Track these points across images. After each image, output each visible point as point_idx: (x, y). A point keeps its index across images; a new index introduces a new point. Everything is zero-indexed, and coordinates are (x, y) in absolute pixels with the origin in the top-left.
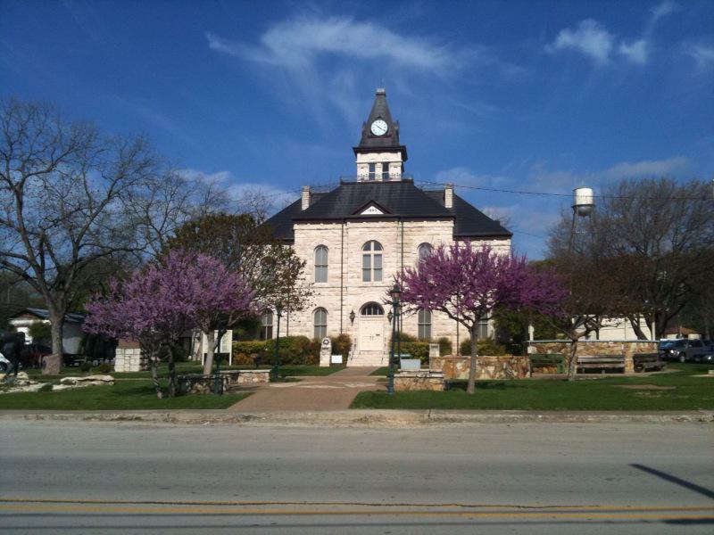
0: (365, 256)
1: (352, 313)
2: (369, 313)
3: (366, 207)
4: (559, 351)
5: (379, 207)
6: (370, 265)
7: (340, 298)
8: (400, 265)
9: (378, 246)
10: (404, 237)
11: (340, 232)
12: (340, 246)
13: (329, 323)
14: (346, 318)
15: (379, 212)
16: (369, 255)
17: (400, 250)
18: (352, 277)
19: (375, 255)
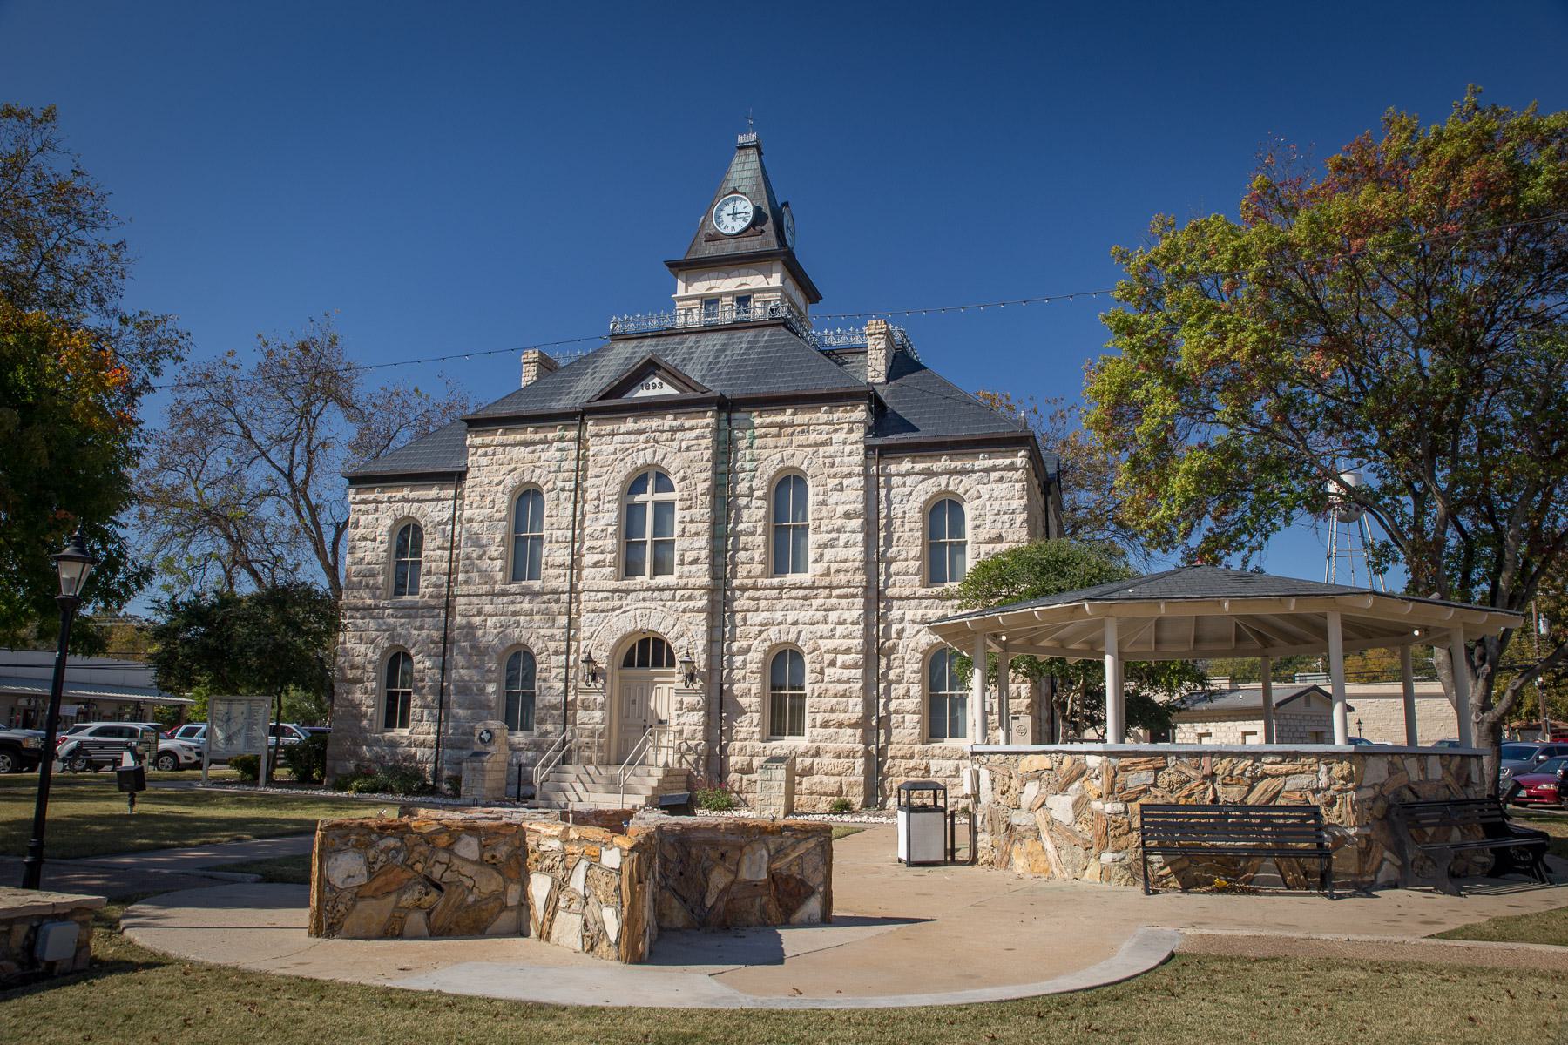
2: (643, 663)
5: (674, 376)
9: (663, 482)
15: (668, 390)
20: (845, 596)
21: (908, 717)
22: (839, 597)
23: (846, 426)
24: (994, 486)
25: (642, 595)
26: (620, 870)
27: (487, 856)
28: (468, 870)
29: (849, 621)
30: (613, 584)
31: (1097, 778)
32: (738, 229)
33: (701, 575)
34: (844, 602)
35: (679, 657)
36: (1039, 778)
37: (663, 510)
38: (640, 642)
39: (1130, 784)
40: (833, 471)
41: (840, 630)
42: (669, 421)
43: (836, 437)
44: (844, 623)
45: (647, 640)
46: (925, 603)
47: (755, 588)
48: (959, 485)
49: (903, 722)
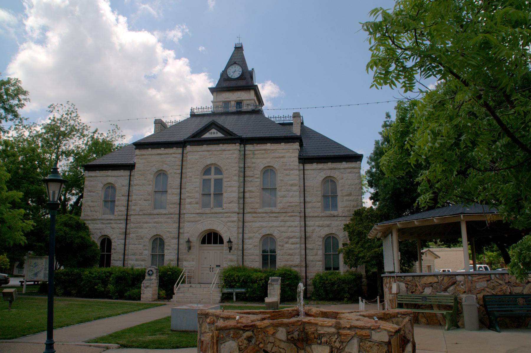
0: (204, 180)
1: (189, 241)
2: (209, 242)
3: (206, 129)
4: (445, 290)
5: (221, 129)
6: (210, 190)
7: (177, 225)
8: (242, 190)
9: (219, 171)
10: (248, 160)
11: (180, 156)
12: (179, 171)
13: (166, 252)
14: (183, 247)
15: (220, 135)
16: (210, 180)
17: (242, 174)
18: (190, 203)
19: (216, 180)
20: (292, 216)
21: (318, 263)
22: (289, 216)
23: (291, 151)
24: (348, 175)
25: (210, 215)
26: (389, 343)
27: (289, 337)
28: (283, 345)
29: (294, 226)
30: (198, 211)
31: (462, 285)
32: (236, 77)
33: (235, 207)
34: (292, 218)
35: (225, 240)
36: (432, 286)
37: (219, 183)
38: (208, 234)
39: (478, 287)
40: (286, 168)
41: (290, 229)
42: (221, 147)
43: (288, 155)
44: (292, 226)
45: (211, 233)
46: (323, 218)
47: (255, 213)
48: (336, 174)
49: (315, 265)
